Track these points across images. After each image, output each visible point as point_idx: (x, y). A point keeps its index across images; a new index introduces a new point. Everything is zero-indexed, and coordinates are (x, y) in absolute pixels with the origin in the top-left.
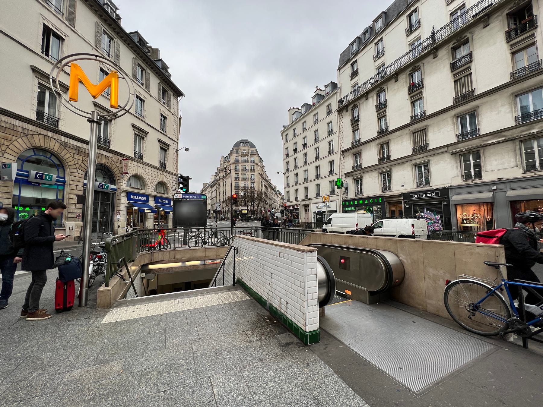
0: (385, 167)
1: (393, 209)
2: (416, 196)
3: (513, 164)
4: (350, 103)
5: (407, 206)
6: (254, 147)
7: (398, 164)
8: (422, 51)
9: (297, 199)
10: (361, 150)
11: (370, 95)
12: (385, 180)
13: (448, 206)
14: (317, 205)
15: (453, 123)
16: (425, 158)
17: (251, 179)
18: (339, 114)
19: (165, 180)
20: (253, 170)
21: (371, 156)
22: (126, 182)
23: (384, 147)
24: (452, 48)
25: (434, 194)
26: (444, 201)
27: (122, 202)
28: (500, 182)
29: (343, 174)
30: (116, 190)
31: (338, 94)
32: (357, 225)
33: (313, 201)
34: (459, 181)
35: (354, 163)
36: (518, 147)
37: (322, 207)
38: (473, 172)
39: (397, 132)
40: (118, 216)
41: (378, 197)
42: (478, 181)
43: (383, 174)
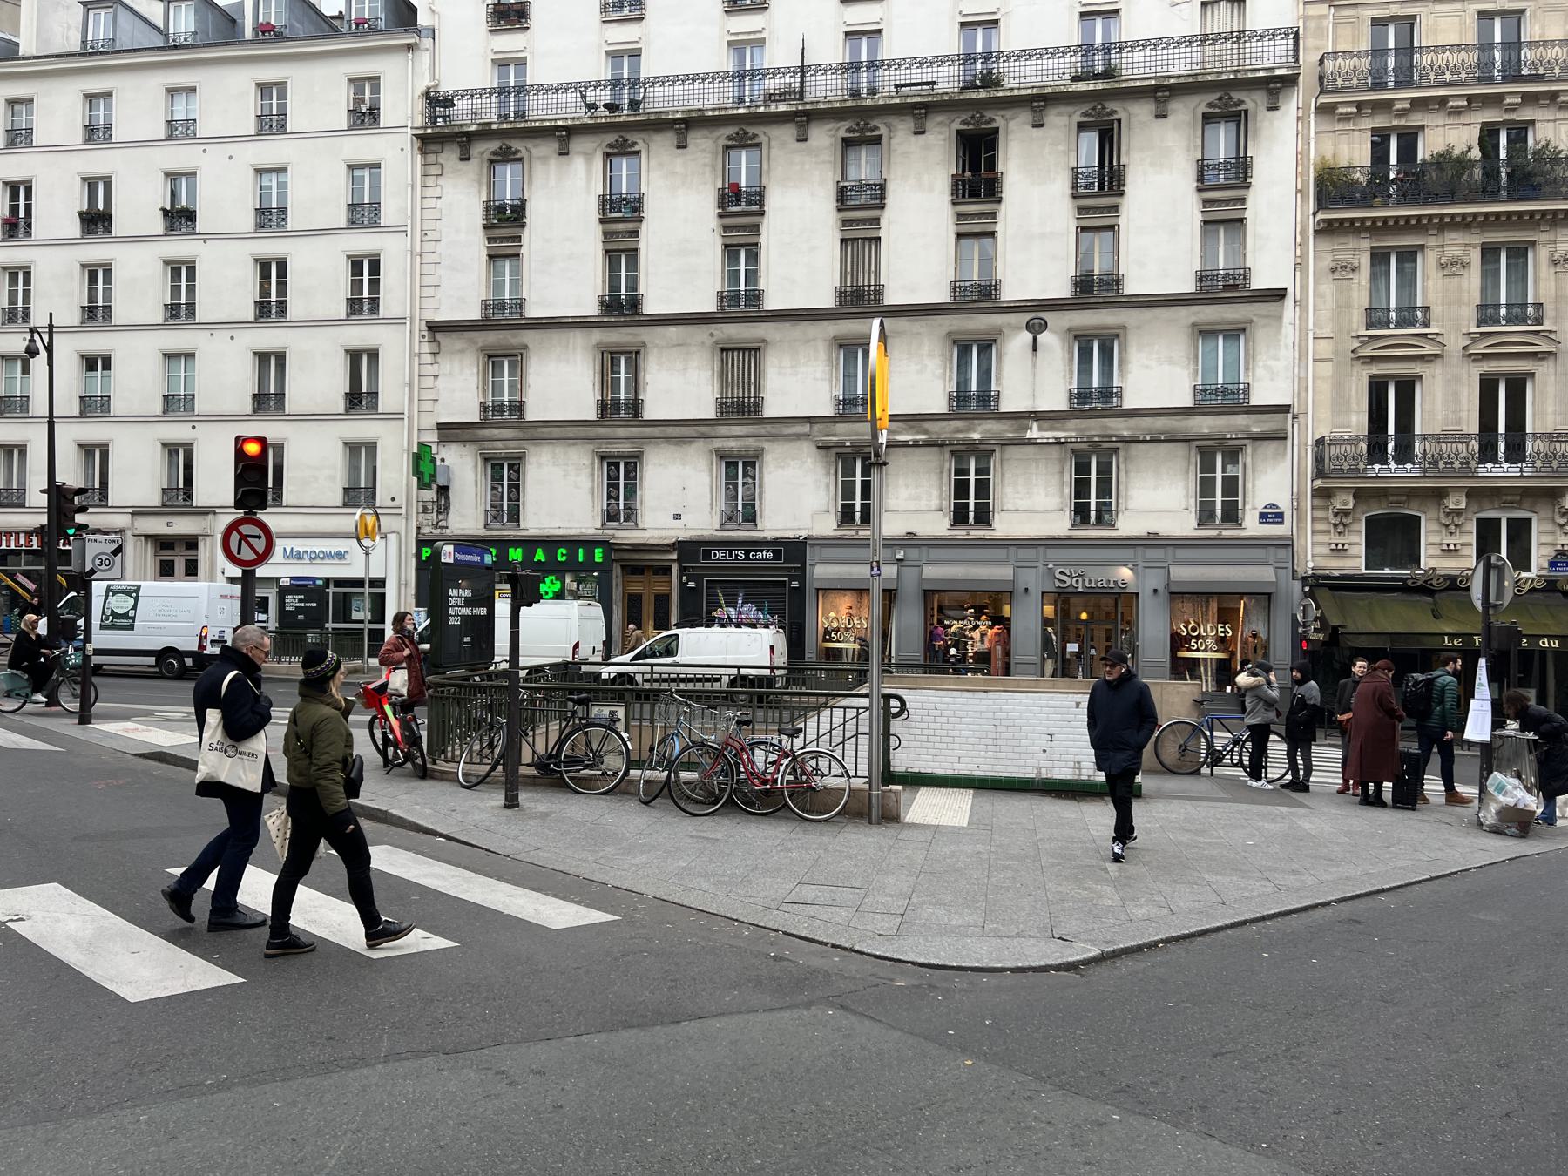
0: (621, 439)
1: (636, 588)
3: (934, 503)
4: (485, 133)
5: (692, 585)
7: (668, 439)
8: (770, 98)
11: (578, 144)
12: (613, 484)
13: (800, 593)
15: (830, 359)
16: (751, 441)
18: (423, 152)
21: (562, 384)
23: (619, 365)
24: (844, 139)
25: (770, 555)
26: (792, 578)
28: (910, 541)
29: (430, 422)
31: (426, 58)
32: (577, 646)
34: (827, 526)
35: (485, 391)
36: (947, 465)
38: (856, 509)
39: (673, 329)
41: (590, 544)
43: (610, 462)
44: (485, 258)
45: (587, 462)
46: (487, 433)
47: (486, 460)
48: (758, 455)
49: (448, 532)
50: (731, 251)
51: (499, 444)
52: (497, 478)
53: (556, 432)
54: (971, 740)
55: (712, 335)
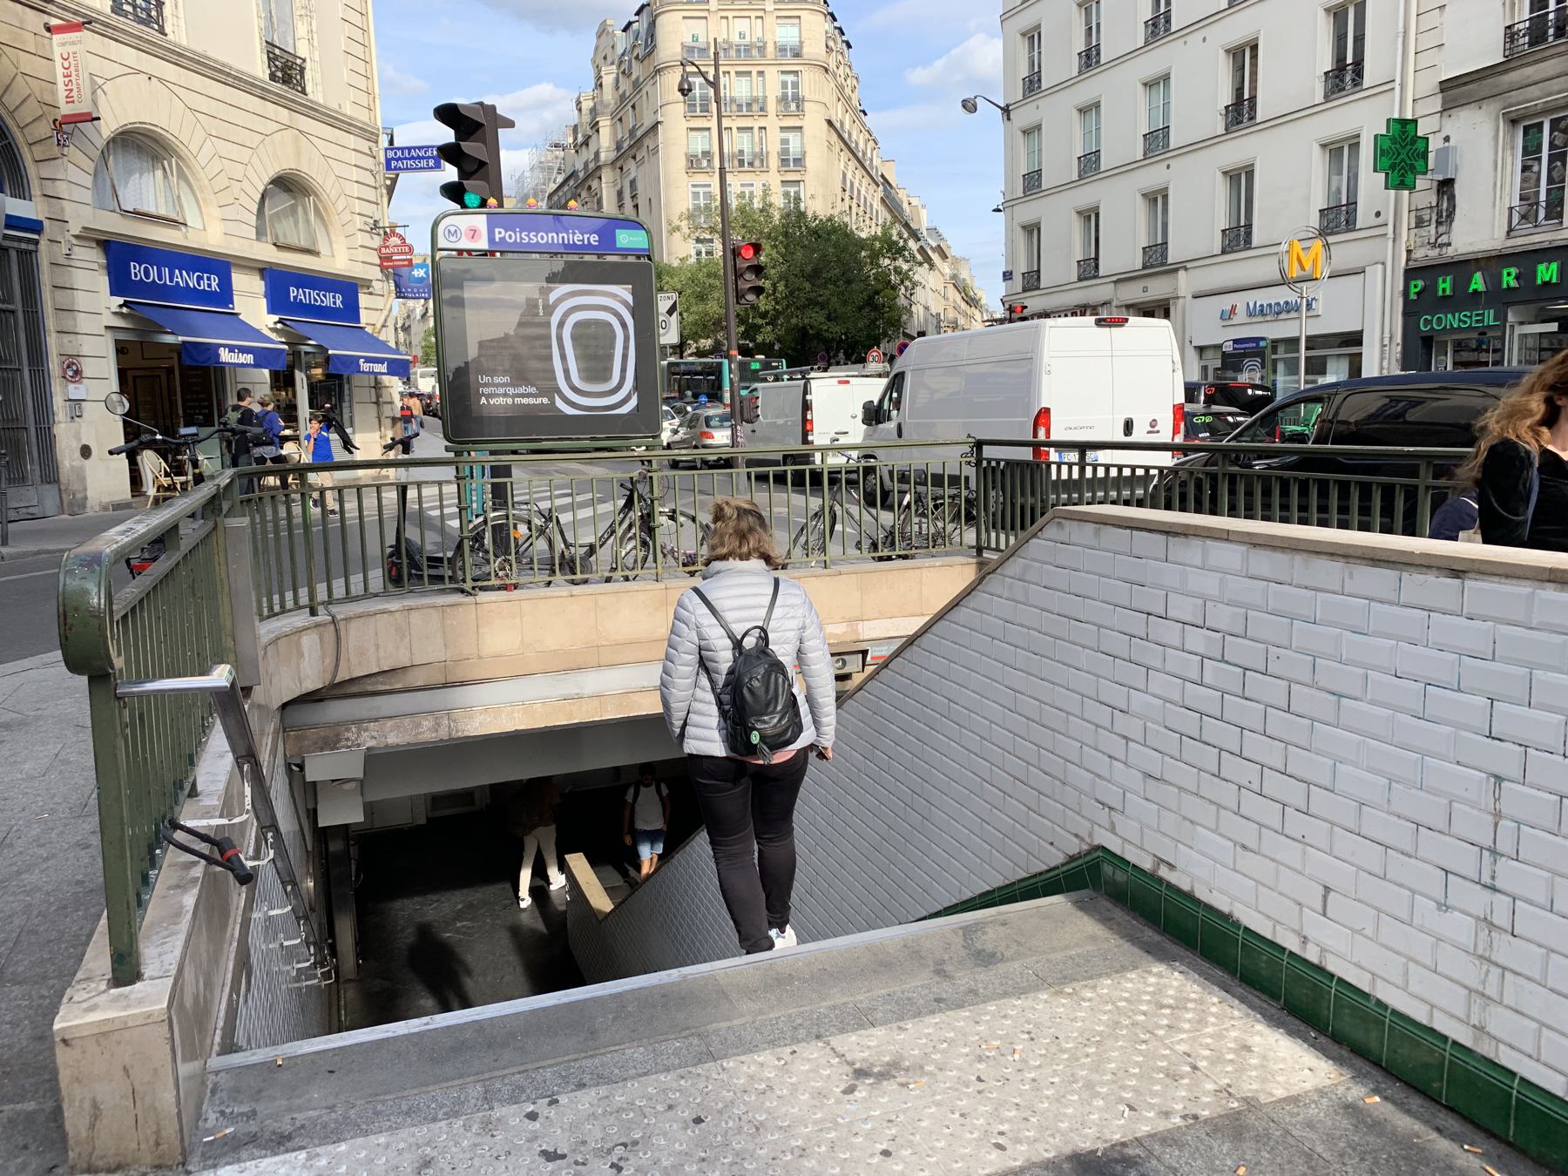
14: (1226, 302)
17: (785, 162)
19: (311, 167)
20: (793, 102)
22: (88, 181)
27: (81, 301)
29: (1431, 82)
30: (35, 227)
37: (1259, 312)
40: (75, 391)
46: (1514, 77)
49: (1450, 251)
51: (1533, 91)
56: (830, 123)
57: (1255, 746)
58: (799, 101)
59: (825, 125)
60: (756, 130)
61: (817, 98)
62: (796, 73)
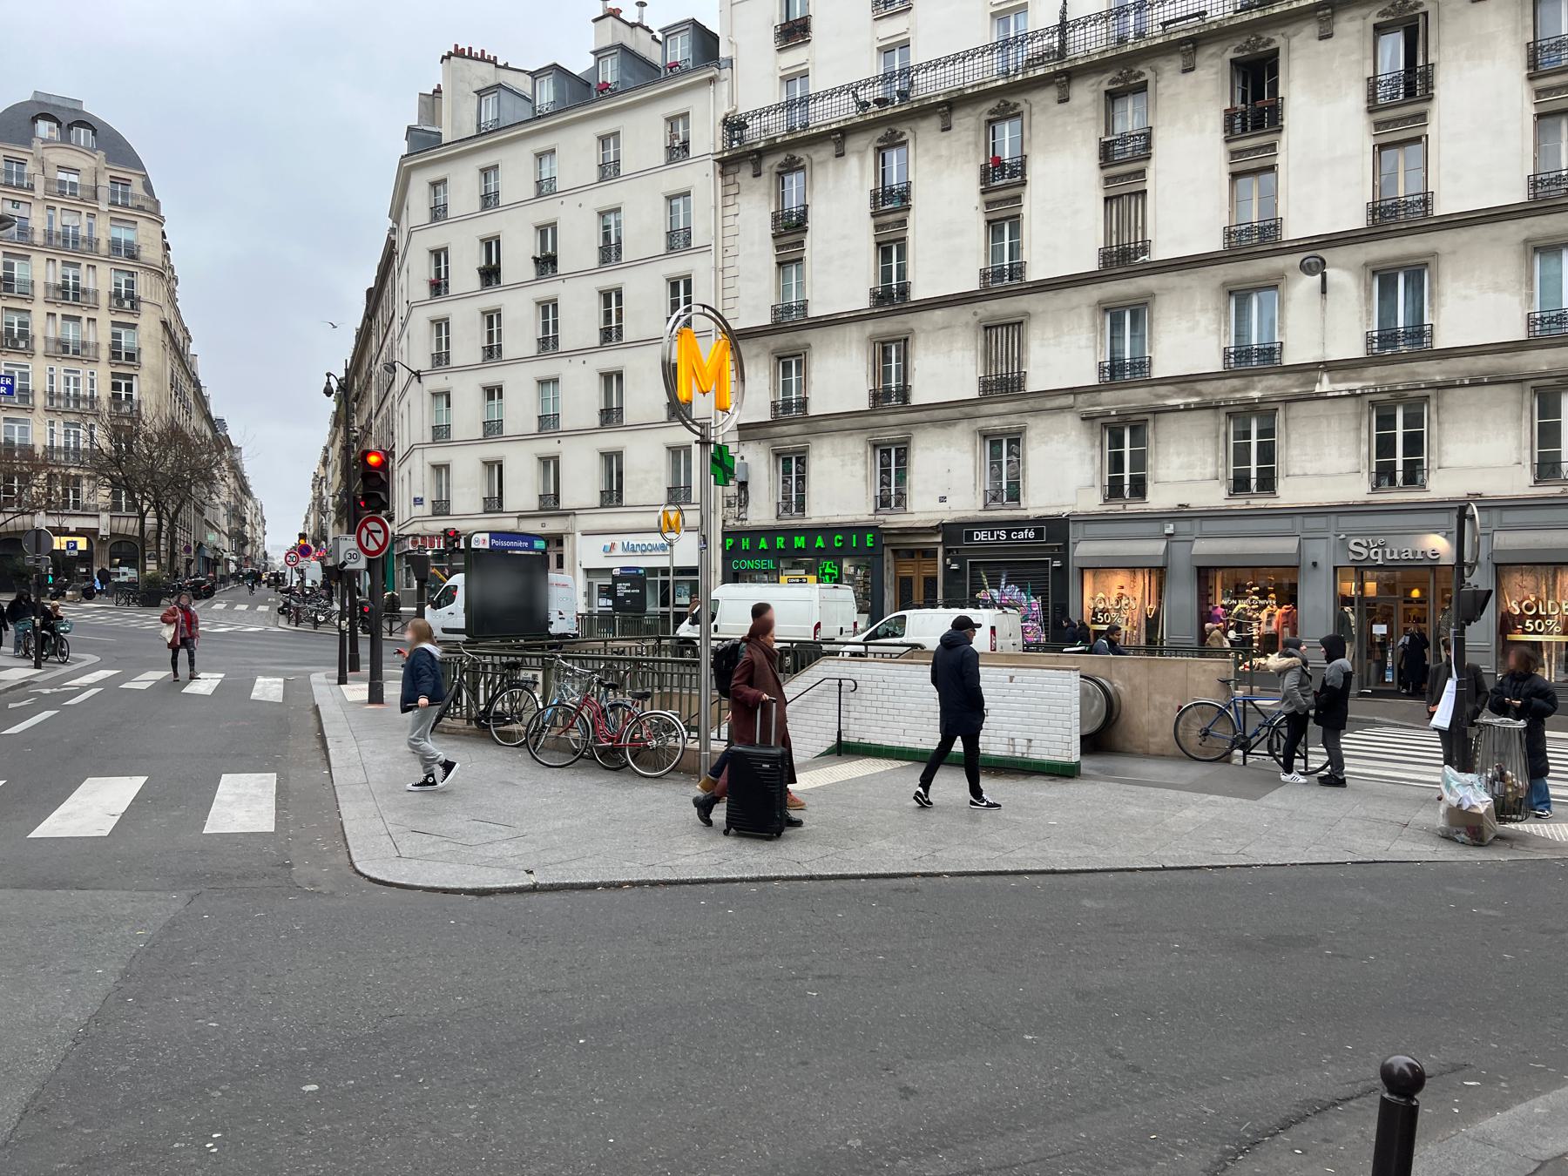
0: (890, 425)
1: (907, 571)
2: (981, 536)
3: (1209, 471)
4: (772, 148)
5: (955, 567)
6: (134, 162)
7: (934, 422)
8: (1031, 63)
9: (494, 504)
10: (809, 346)
11: (853, 144)
12: (885, 472)
13: (1063, 572)
14: (607, 540)
15: (1094, 325)
16: (1014, 419)
17: (115, 355)
18: (723, 174)
20: (126, 300)
21: (840, 378)
23: (890, 355)
24: (1107, 92)
25: (1032, 534)
26: (1055, 558)
28: (1182, 514)
31: (724, 88)
32: (818, 626)
33: (584, 522)
34: (1093, 502)
35: (775, 391)
36: (1223, 429)
37: (631, 549)
38: (1127, 480)
41: (861, 530)
42: (1134, 507)
44: (774, 265)
45: (861, 451)
46: (777, 429)
47: (777, 455)
48: (1021, 431)
50: (994, 226)
51: (787, 440)
52: (787, 471)
53: (834, 424)
54: (915, 713)
55: (975, 314)
56: (164, 323)
57: (886, 705)
58: (135, 301)
59: (160, 327)
60: (84, 321)
61: (152, 300)
62: (132, 274)
